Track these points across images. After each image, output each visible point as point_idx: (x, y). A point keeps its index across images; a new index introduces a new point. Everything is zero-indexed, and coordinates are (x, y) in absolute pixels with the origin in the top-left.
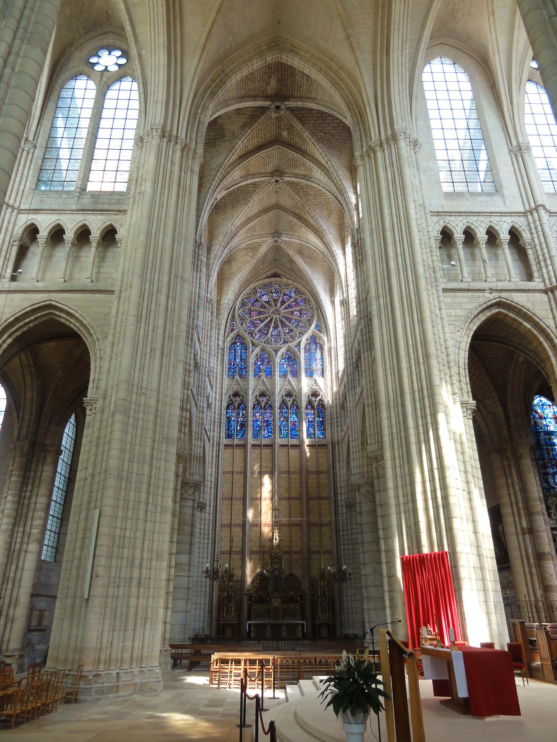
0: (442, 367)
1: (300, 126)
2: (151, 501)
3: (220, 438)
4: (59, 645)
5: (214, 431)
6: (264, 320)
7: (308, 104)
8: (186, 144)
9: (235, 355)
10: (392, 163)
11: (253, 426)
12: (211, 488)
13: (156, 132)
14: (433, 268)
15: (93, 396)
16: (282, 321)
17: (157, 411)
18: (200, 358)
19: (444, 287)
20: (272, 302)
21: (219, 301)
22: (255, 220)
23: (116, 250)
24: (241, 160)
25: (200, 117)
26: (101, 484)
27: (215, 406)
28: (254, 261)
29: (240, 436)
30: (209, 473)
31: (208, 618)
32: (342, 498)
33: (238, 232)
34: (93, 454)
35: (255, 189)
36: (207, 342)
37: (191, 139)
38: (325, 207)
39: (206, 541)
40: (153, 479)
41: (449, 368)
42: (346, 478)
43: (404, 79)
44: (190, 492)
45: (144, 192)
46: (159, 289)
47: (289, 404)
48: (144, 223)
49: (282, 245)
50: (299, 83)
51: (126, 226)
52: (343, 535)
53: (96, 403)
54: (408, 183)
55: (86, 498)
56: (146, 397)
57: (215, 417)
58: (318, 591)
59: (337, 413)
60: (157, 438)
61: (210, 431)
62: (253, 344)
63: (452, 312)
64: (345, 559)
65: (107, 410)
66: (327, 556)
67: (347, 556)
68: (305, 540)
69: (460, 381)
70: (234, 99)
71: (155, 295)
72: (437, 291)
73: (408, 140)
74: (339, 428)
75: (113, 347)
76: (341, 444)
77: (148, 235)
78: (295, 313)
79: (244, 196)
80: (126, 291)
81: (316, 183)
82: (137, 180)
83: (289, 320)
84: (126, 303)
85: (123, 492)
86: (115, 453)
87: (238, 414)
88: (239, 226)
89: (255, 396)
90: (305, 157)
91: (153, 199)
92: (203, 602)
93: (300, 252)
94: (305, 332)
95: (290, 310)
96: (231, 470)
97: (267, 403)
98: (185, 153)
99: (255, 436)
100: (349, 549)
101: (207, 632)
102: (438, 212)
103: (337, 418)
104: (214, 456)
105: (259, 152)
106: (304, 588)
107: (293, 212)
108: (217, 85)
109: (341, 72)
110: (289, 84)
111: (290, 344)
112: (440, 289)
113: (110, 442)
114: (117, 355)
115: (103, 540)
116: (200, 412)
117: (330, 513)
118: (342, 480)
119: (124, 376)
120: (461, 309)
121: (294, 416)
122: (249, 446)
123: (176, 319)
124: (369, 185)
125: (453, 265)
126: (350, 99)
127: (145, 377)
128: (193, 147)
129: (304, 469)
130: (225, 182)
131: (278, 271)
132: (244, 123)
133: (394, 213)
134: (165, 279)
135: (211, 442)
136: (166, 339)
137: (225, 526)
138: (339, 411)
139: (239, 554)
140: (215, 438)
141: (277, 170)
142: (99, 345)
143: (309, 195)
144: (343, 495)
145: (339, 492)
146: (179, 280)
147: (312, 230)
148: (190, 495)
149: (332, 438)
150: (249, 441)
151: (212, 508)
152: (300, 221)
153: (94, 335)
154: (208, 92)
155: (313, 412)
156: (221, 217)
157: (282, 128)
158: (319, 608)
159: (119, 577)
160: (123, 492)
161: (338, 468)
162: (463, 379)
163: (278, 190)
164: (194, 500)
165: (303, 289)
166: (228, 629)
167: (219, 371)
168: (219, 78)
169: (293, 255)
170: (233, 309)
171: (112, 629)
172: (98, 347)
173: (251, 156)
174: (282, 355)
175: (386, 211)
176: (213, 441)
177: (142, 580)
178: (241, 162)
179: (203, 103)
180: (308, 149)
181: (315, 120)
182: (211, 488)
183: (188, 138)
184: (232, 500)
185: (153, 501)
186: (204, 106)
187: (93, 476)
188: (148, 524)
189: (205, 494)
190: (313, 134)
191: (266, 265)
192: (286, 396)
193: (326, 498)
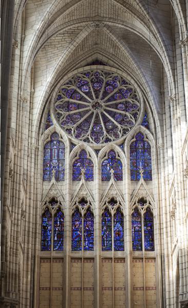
3: (35, 250)
5: (28, 243)
11: (72, 236)
18: (14, 164)
21: (32, 95)
22: (74, 5)
33: (56, 19)
42: (175, 295)
57: (29, 227)
61: (24, 242)
74: (169, 239)
78: (120, 106)
96: (48, 286)
99: (75, 247)
104: (30, 270)
116: (14, 224)
122: (68, 260)
129: (129, 285)
131: (100, 57)
138: (168, 220)
140: (30, 250)
147: (138, 17)
152: (125, 6)
165: (129, 78)
176: (28, 254)
191: (86, 50)
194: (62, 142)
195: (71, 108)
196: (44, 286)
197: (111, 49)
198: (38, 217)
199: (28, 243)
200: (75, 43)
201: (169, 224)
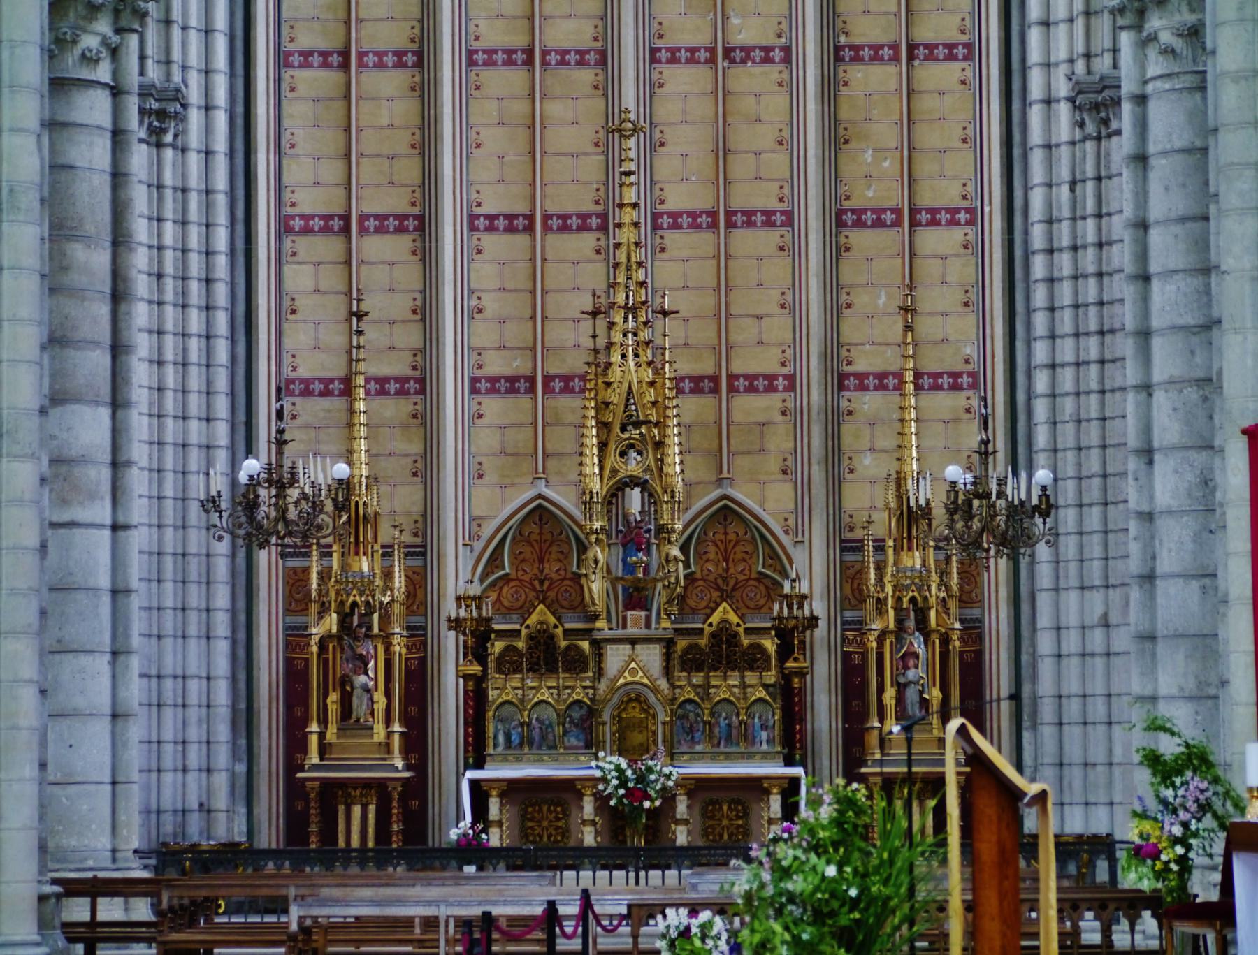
31: (234, 756)
39: (195, 321)
44: (90, 42)
52: (1051, 280)
58: (881, 603)
66: (944, 403)
67: (1068, 405)
139: (401, 392)
144: (1061, 32)
148: (89, 59)
151: (221, 119)
158: (890, 695)
164: (116, 91)
166: (357, 810)
184: (345, 66)
189: (176, 32)
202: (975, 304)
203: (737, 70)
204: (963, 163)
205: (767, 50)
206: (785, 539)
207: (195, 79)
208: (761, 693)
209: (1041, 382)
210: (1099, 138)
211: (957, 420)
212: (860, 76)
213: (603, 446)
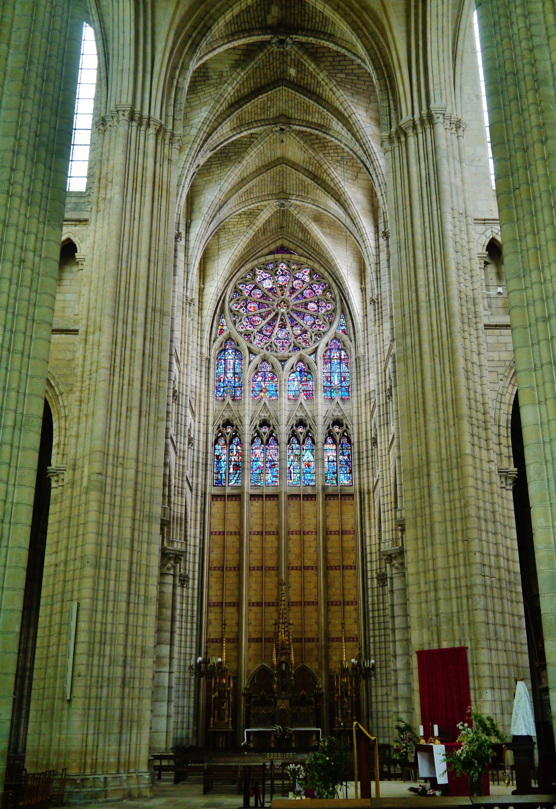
0: (475, 429)
1: (313, 65)
2: (133, 591)
3: (206, 485)
4: (38, 750)
5: (197, 477)
6: (267, 316)
7: (323, 42)
8: (161, 126)
9: (225, 368)
10: (426, 155)
12: (194, 554)
13: (124, 115)
14: (474, 299)
15: (59, 465)
16: (291, 317)
17: (136, 483)
18: (179, 383)
19: (487, 322)
20: (279, 289)
21: (201, 291)
22: (251, 180)
23: (75, 269)
24: (233, 109)
25: (177, 82)
26: (78, 572)
27: (199, 441)
28: (251, 233)
29: (233, 481)
30: (192, 535)
32: (373, 568)
33: (229, 199)
34: (65, 536)
35: (252, 139)
36: (188, 360)
37: (167, 115)
38: (350, 164)
39: (189, 626)
40: (134, 566)
41: (486, 429)
42: (377, 541)
43: (446, 33)
44: (169, 565)
45: (111, 200)
46: (134, 330)
47: (301, 438)
48: (113, 246)
49: (291, 210)
50: (310, 13)
51: (89, 241)
53: (63, 473)
54: (446, 187)
55: (59, 588)
56: (123, 468)
57: (198, 457)
58: (338, 690)
59: (367, 451)
60: (137, 517)
61: (193, 476)
62: (251, 352)
63: (495, 355)
64: (374, 649)
65: (78, 484)
66: (351, 644)
67: (378, 645)
68: (323, 625)
69: (500, 444)
70: (222, 38)
71: (129, 338)
72: (477, 330)
73: (448, 122)
74: (370, 471)
75: (80, 405)
76: (372, 495)
77: (119, 259)
79: (236, 150)
80: (94, 333)
81: (336, 139)
82: (100, 179)
83: (302, 315)
84: (96, 350)
85: (102, 582)
86: (91, 537)
87: (230, 451)
88: (230, 191)
89: (253, 427)
90: (320, 105)
91: (123, 209)
92: (186, 704)
93: (318, 219)
94: (324, 333)
95: (304, 300)
96: (222, 530)
97: (271, 435)
98: (160, 137)
100: (380, 636)
101: (192, 742)
102: (485, 220)
103: (367, 457)
104: (199, 510)
105: (257, 96)
106: (321, 686)
107: (305, 169)
108: (199, 33)
109: (364, 14)
110: (296, 12)
111: (302, 352)
112: (481, 326)
113: (85, 524)
114: (87, 416)
115: (83, 637)
116: (180, 457)
117: (356, 587)
118: (373, 542)
119: (98, 444)
120: (507, 351)
121: (308, 453)
122: (246, 497)
123: (155, 366)
124: (399, 180)
125: (499, 293)
126: (376, 53)
127: (122, 444)
128: (170, 127)
130: (210, 141)
131: (286, 243)
132: (236, 60)
133: (427, 224)
134: (141, 316)
135: (194, 492)
136: (145, 393)
137: (214, 606)
138: (370, 448)
139: (233, 642)
140: (200, 486)
141: (282, 115)
142: (63, 401)
143: (328, 148)
144: (374, 563)
145: (369, 559)
146: (158, 314)
147: (332, 196)
148: (169, 569)
149: (360, 484)
150: (246, 490)
151: (196, 582)
152: (315, 182)
153: (56, 388)
154: (188, 45)
155: (334, 447)
156: (205, 179)
157: (289, 63)
158: (340, 711)
159: (102, 677)
160: (102, 582)
161: (367, 526)
162: (504, 441)
163: (284, 140)
164: (174, 576)
166: (221, 739)
167: (203, 391)
168: (202, 23)
169: (308, 223)
170: (221, 301)
171: (96, 731)
172: (61, 403)
173: (246, 103)
174: (292, 368)
175: (418, 222)
176: (197, 490)
177: (127, 680)
178: (233, 113)
179: (181, 61)
180: (324, 93)
181: (333, 57)
182: (194, 554)
183: (163, 117)
184: (223, 570)
185: (135, 591)
186: (183, 63)
187: (66, 562)
188: (131, 617)
189: (188, 563)
190: (331, 76)
191: (269, 234)
192: (297, 426)
193: (351, 567)
194: (238, 351)
195: (250, 307)
196: (217, 530)
197: (300, 234)
198: (210, 444)
199: (197, 477)
200: (254, 228)
201: (370, 452)
202: (357, 622)
203: (306, 571)
204: (354, 592)
205: (312, 567)
206: (317, 675)
207: (191, 573)
208: (311, 711)
209: (372, 640)
210: (383, 586)
211: (353, 648)
212: (332, 573)
213: (277, 654)
